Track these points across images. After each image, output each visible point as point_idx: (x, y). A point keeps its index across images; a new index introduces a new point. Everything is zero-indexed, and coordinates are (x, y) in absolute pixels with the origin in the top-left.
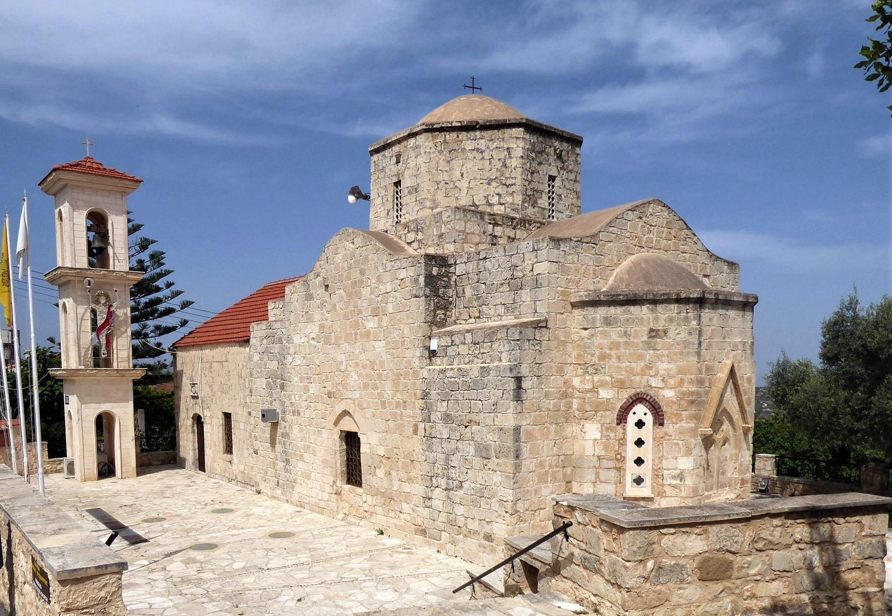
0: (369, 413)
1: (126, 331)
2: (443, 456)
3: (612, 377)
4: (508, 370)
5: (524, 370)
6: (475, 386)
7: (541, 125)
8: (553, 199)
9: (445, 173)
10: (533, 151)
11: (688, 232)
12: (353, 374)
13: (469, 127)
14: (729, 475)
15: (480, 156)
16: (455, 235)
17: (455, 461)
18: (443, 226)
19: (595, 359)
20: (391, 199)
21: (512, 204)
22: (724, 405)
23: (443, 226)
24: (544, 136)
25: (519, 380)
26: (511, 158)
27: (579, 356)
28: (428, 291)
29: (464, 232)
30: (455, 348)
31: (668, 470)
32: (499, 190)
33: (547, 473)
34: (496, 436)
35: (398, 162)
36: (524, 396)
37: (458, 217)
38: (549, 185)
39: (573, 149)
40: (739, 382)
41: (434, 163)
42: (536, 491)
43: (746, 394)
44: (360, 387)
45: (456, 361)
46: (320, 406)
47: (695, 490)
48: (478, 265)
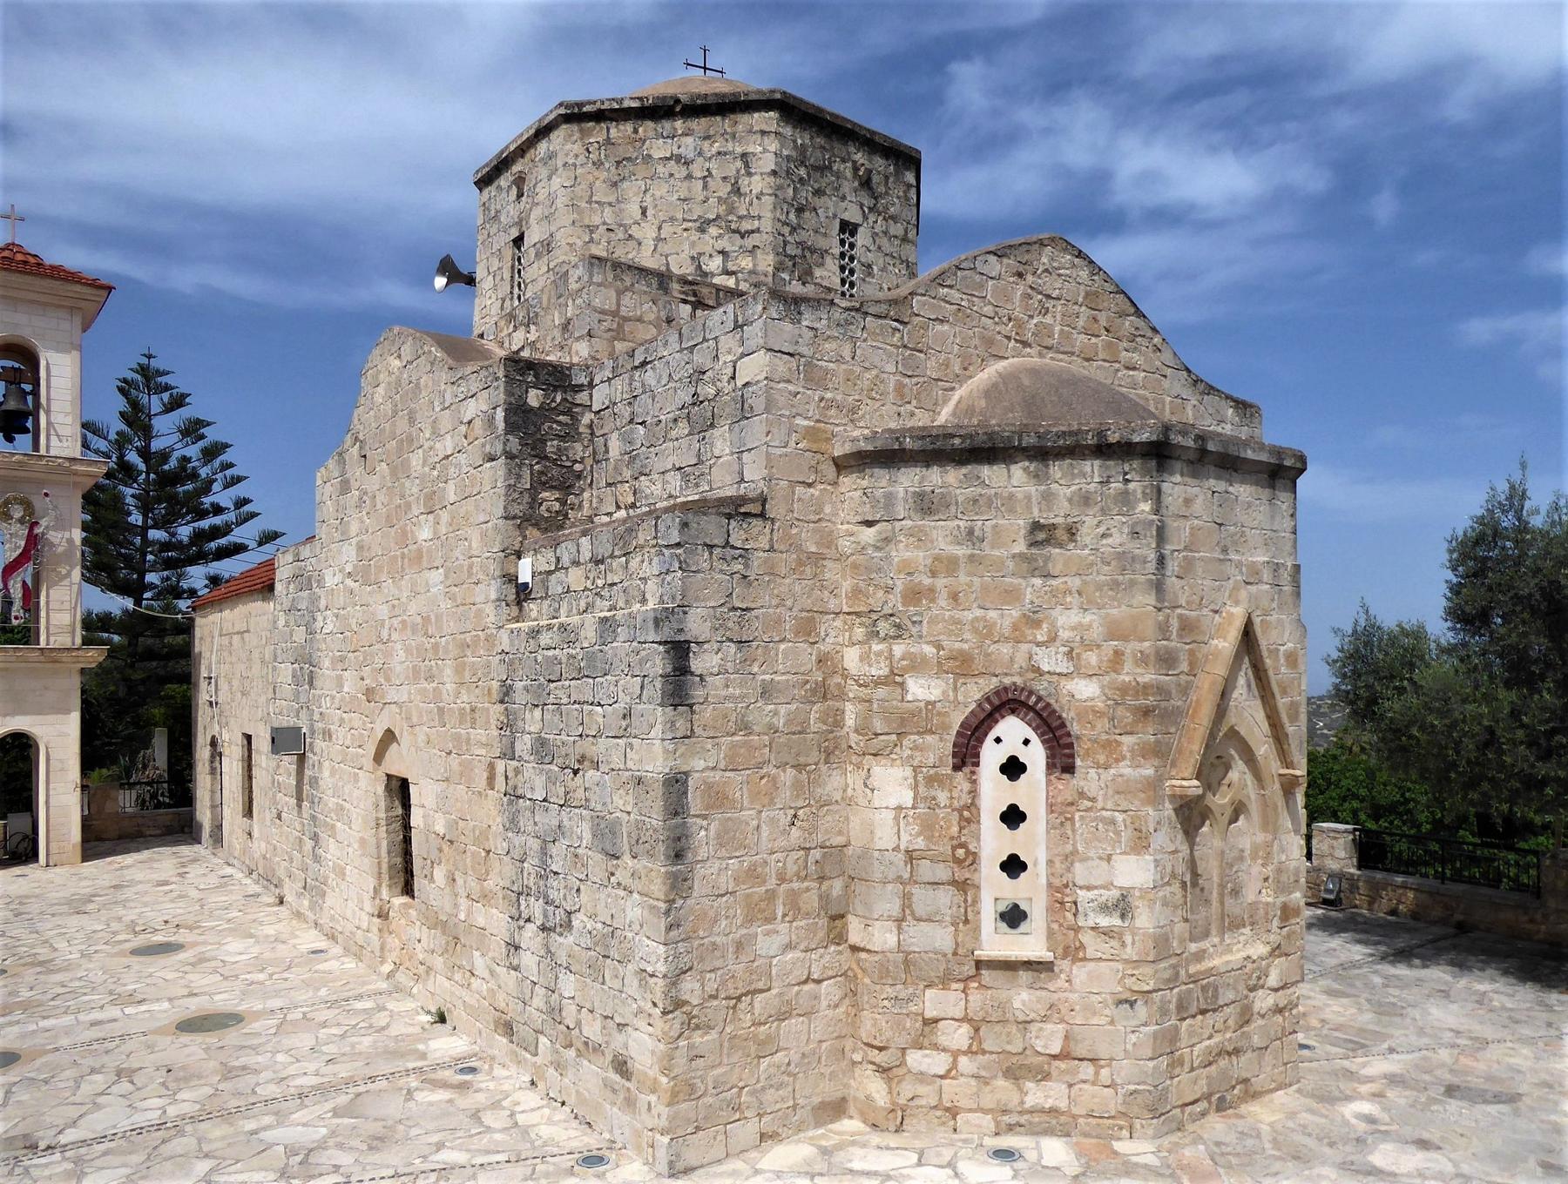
0: (422, 733)
1: (68, 575)
3: (939, 647)
4: (651, 624)
5: (696, 624)
7: (821, 110)
8: (852, 272)
9: (607, 210)
10: (802, 163)
11: (1140, 323)
12: (399, 646)
13: (658, 111)
14: (1250, 895)
15: (684, 173)
16: (590, 320)
18: (570, 303)
19: (895, 601)
20: (507, 275)
21: (753, 272)
22: (1232, 719)
23: (570, 303)
24: (828, 136)
25: (679, 651)
26: (749, 174)
27: (856, 593)
28: (514, 444)
29: (615, 314)
31: (1089, 888)
32: (720, 245)
33: (771, 896)
34: (630, 798)
35: (520, 195)
36: (698, 693)
37: (597, 278)
38: (842, 242)
39: (897, 173)
40: (1268, 661)
41: (583, 186)
42: (739, 946)
43: (1284, 692)
44: (407, 678)
46: (356, 719)
47: (1161, 945)
48: (632, 379)
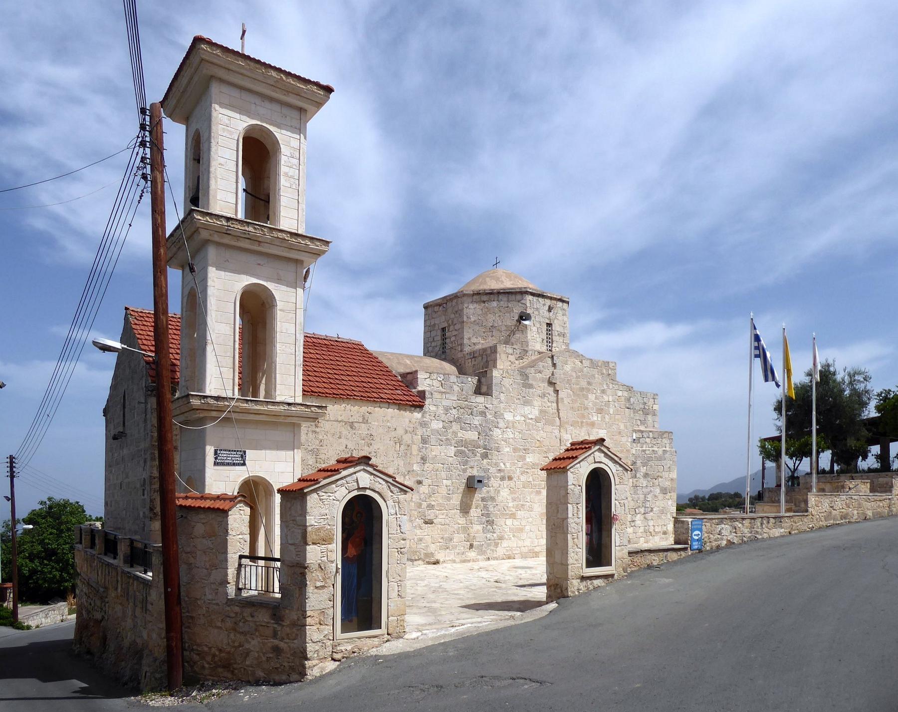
6: (660, 459)
17: (649, 497)
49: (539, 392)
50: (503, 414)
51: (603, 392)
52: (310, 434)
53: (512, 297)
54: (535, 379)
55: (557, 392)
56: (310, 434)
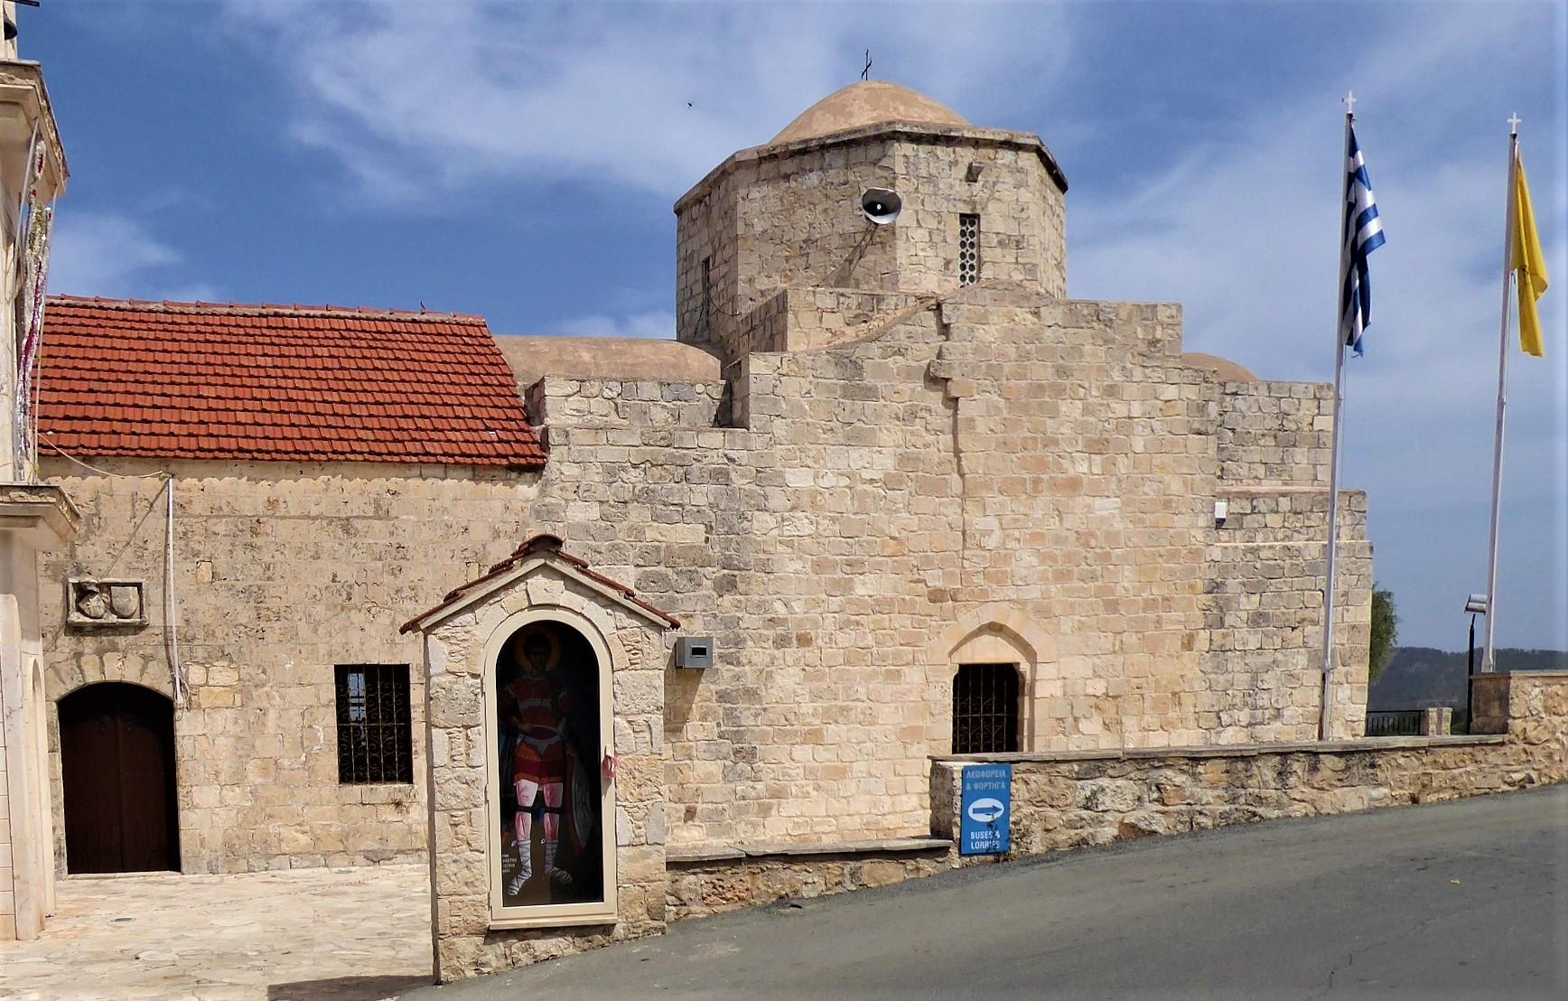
2: (1247, 677)
17: (1270, 680)
30: (1259, 517)
45: (1260, 537)
46: (903, 622)
49: (899, 408)
50: (781, 475)
51: (1111, 391)
52: (239, 552)
53: (857, 154)
54: (882, 372)
55: (953, 402)
56: (239, 552)
